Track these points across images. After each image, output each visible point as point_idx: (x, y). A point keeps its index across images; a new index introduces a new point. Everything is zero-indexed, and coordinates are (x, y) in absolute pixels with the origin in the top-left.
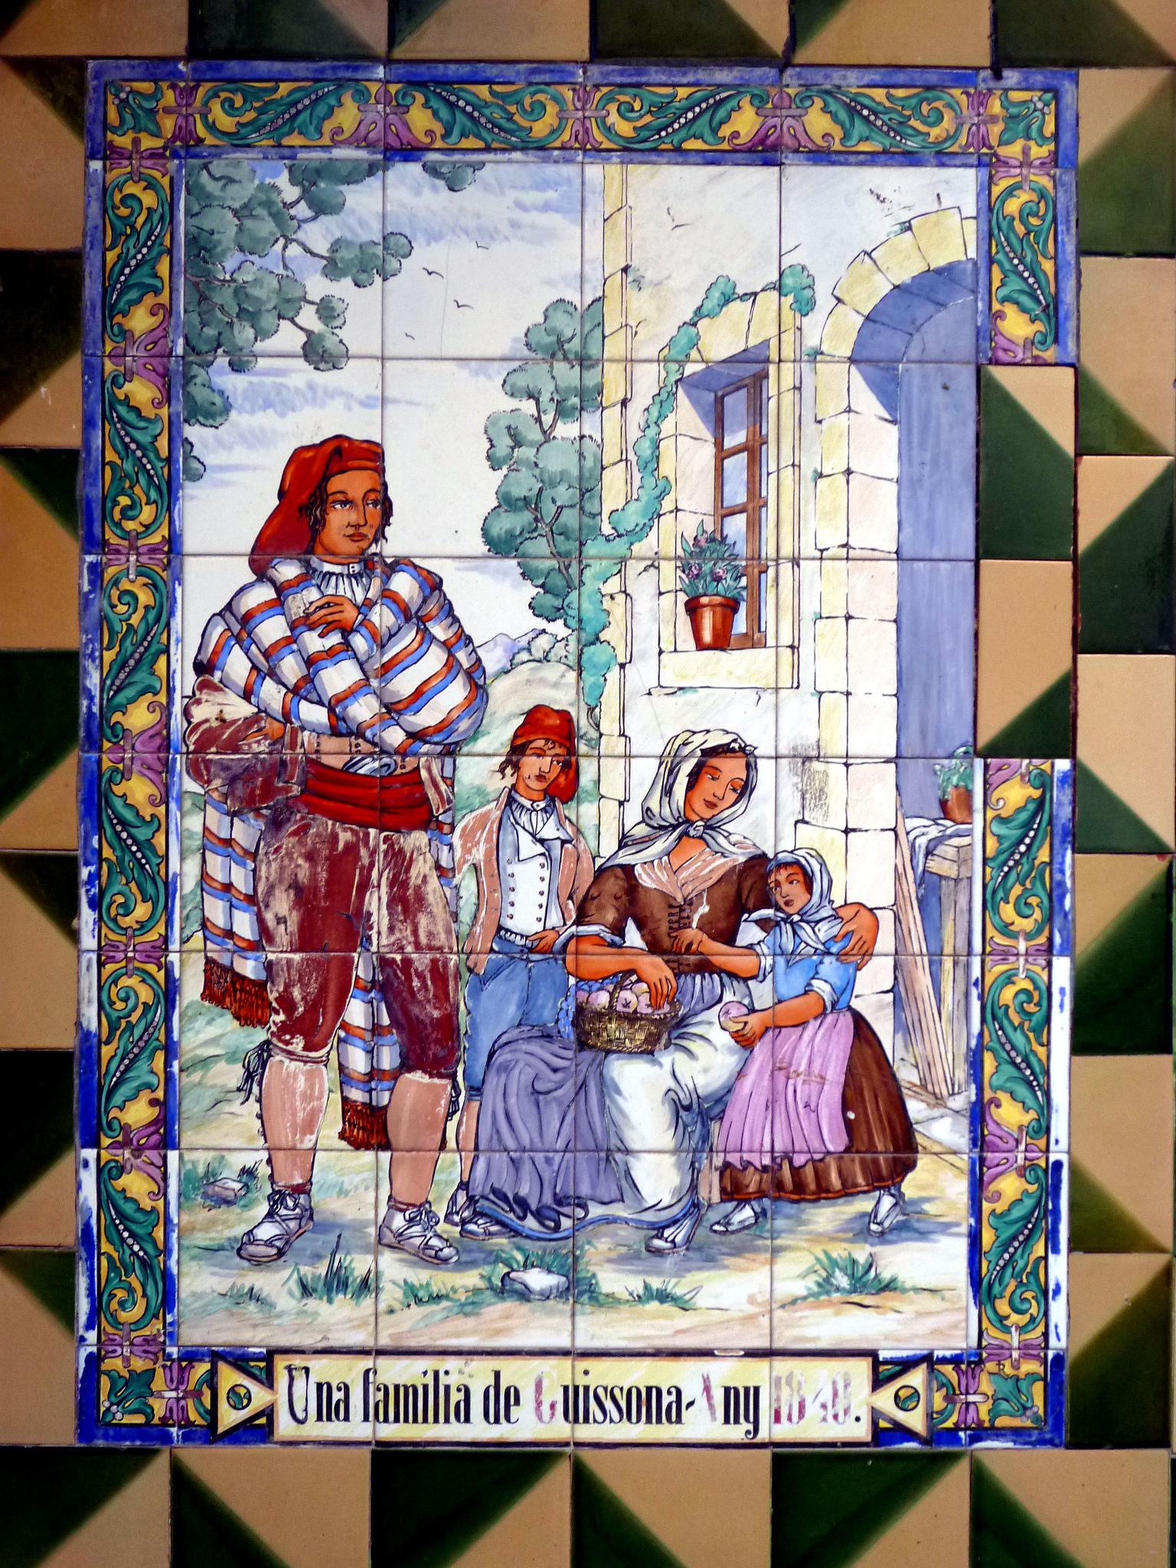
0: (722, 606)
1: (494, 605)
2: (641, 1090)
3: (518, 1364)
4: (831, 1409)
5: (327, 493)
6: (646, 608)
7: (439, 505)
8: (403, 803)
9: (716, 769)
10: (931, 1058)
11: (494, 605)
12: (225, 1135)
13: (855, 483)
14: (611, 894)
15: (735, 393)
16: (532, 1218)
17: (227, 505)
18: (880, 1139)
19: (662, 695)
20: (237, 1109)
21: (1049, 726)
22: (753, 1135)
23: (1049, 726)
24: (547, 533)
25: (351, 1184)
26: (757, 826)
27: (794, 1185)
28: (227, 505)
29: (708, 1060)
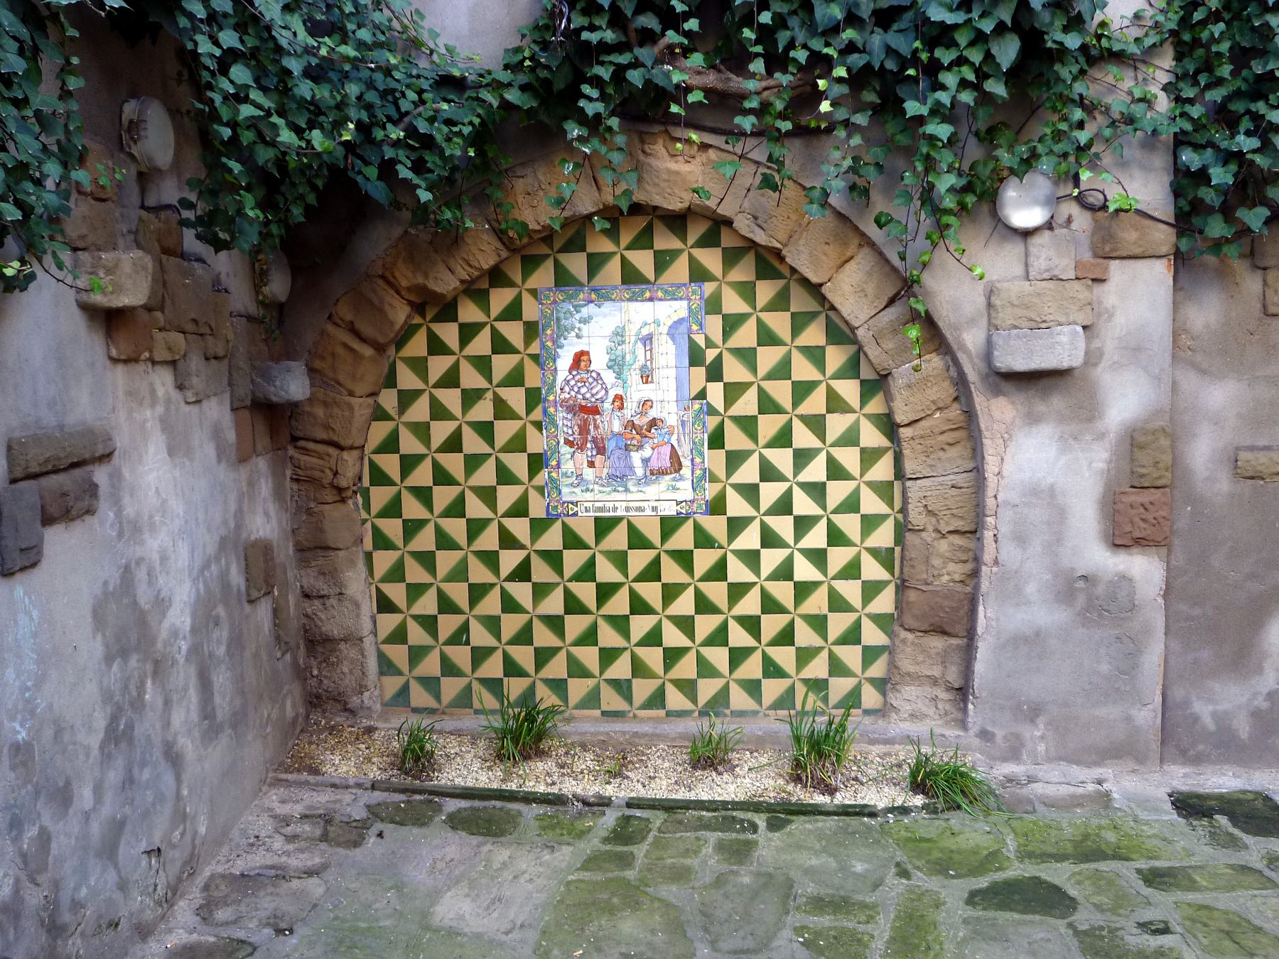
0: (646, 378)
1: (609, 377)
2: (636, 457)
3: (617, 502)
4: (670, 510)
5: (580, 359)
6: (634, 377)
7: (599, 361)
8: (595, 411)
9: (646, 404)
10: (684, 451)
11: (609, 377)
12: (568, 466)
13: (668, 355)
14: (631, 425)
15: (648, 340)
16: (619, 479)
17: (564, 362)
18: (676, 464)
19: (636, 392)
20: (570, 462)
21: (702, 395)
22: (655, 464)
23: (702, 395)
24: (617, 365)
25: (589, 474)
26: (653, 413)
27: (662, 472)
28: (564, 362)
29: (647, 452)
